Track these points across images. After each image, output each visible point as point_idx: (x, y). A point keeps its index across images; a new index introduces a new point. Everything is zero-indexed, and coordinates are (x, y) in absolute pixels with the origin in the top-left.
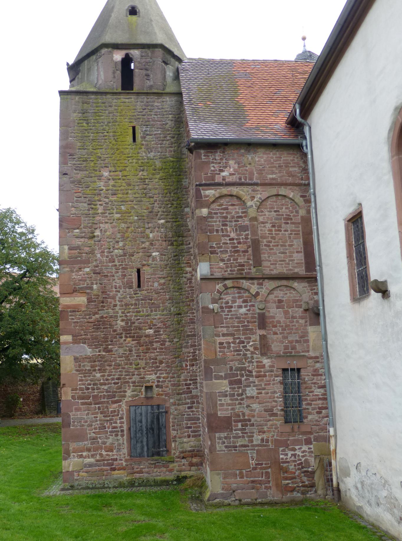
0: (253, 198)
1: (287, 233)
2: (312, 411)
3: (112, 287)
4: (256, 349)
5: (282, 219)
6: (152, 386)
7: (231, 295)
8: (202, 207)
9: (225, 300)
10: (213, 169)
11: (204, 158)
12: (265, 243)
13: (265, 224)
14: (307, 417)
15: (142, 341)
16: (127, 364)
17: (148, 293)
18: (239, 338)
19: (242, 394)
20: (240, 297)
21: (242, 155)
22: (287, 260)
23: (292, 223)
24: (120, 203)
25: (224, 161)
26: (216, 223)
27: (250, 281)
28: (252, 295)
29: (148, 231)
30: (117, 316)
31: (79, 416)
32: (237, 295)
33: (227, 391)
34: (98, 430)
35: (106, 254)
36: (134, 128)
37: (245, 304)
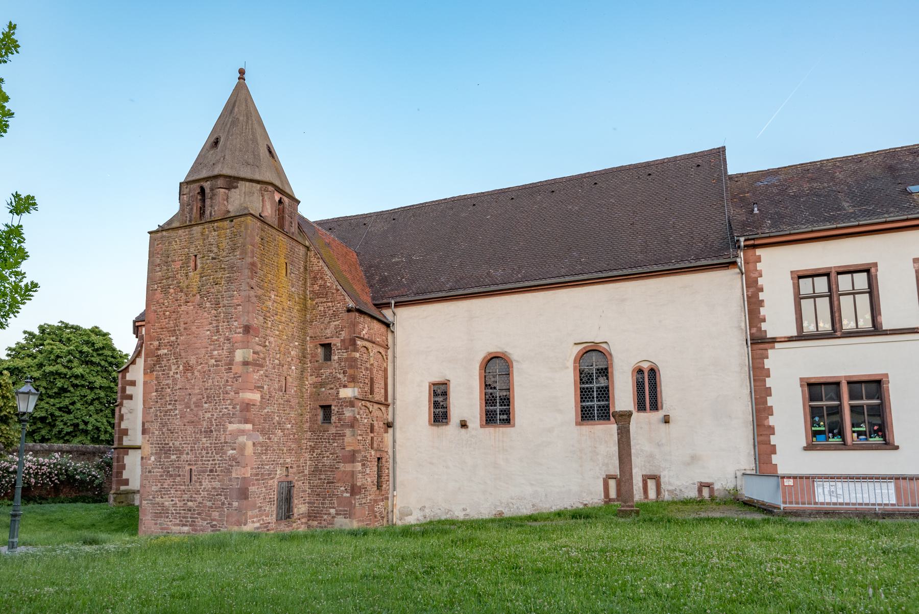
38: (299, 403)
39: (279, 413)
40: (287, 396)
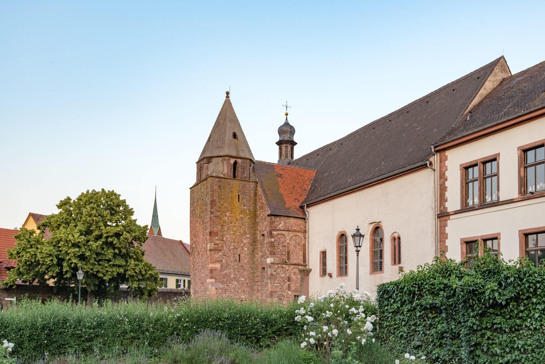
0: (288, 236)
4: (286, 288)
20: (282, 271)
36: (239, 195)
38: (250, 267)
40: (241, 264)
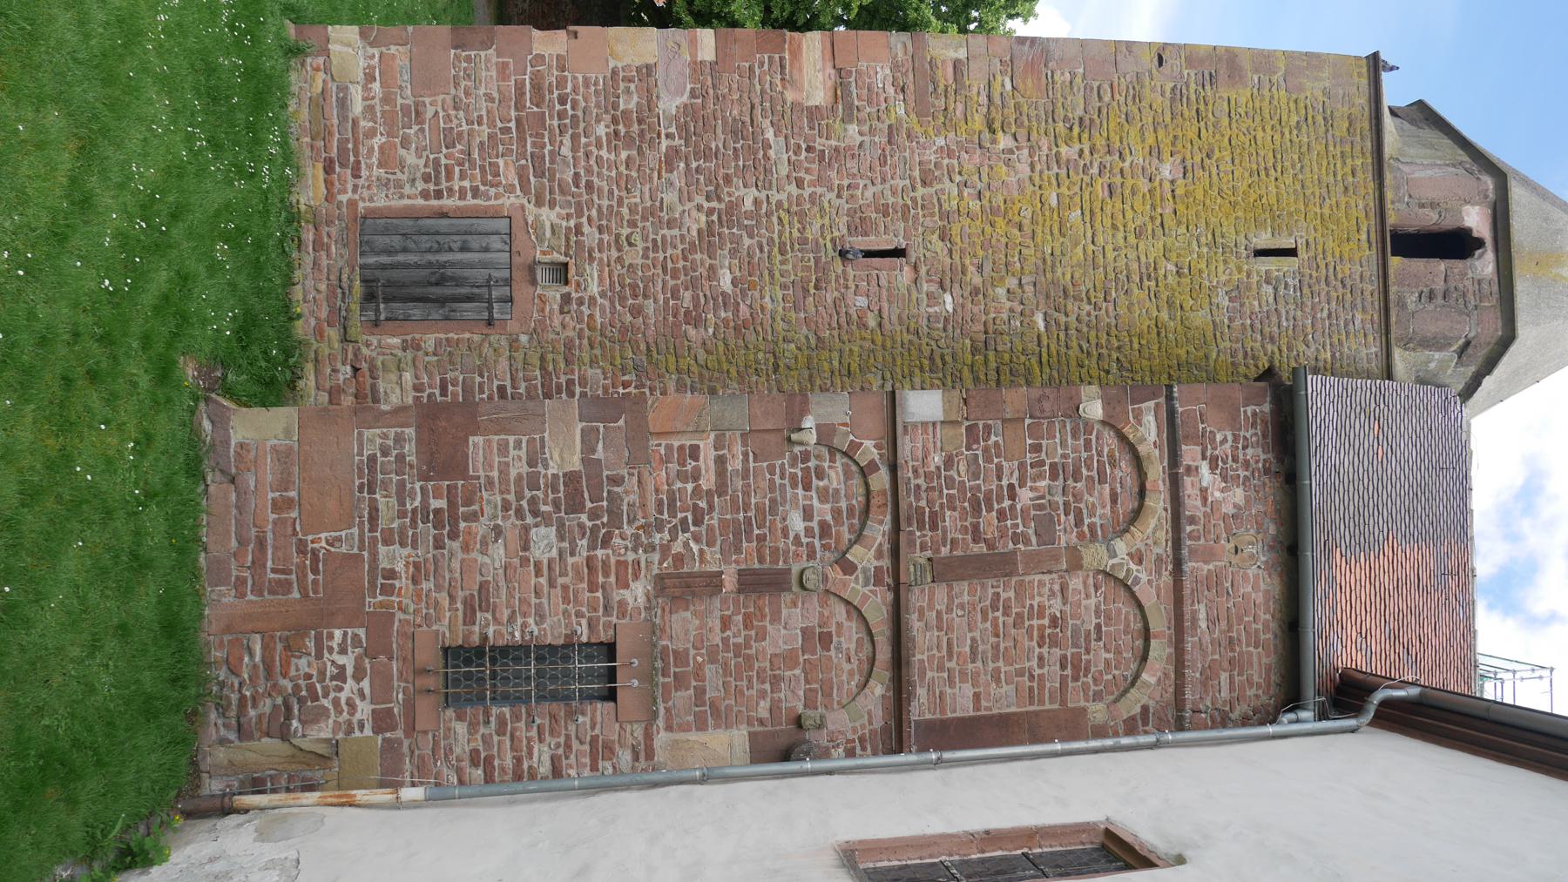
0: (1138, 558)
1: (1035, 663)
2: (479, 737)
3: (854, 175)
4: (679, 559)
5: (1074, 650)
6: (567, 283)
7: (843, 486)
8: (1107, 403)
9: (830, 467)
10: (1219, 437)
11: (1249, 414)
12: (1003, 596)
13: (1059, 594)
14: (460, 718)
15: (698, 256)
16: (633, 209)
17: (837, 277)
18: (711, 508)
19: (535, 513)
20: (837, 513)
21: (1260, 527)
22: (952, 664)
23: (1063, 679)
24: (1087, 206)
25: (1242, 473)
26: (1059, 446)
27: (886, 547)
28: (845, 553)
29: (1012, 282)
30: (770, 188)
31: (484, 74)
32: (843, 504)
33: (546, 467)
34: (442, 125)
35: (946, 161)
37: (817, 531)
39: (768, 215)
